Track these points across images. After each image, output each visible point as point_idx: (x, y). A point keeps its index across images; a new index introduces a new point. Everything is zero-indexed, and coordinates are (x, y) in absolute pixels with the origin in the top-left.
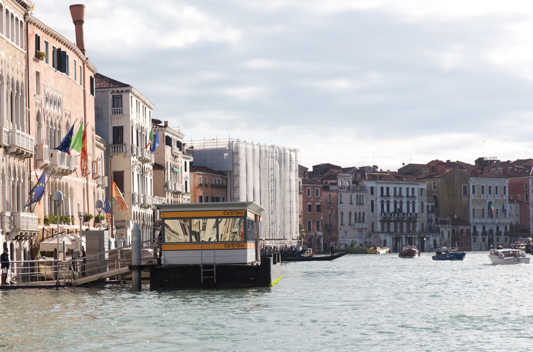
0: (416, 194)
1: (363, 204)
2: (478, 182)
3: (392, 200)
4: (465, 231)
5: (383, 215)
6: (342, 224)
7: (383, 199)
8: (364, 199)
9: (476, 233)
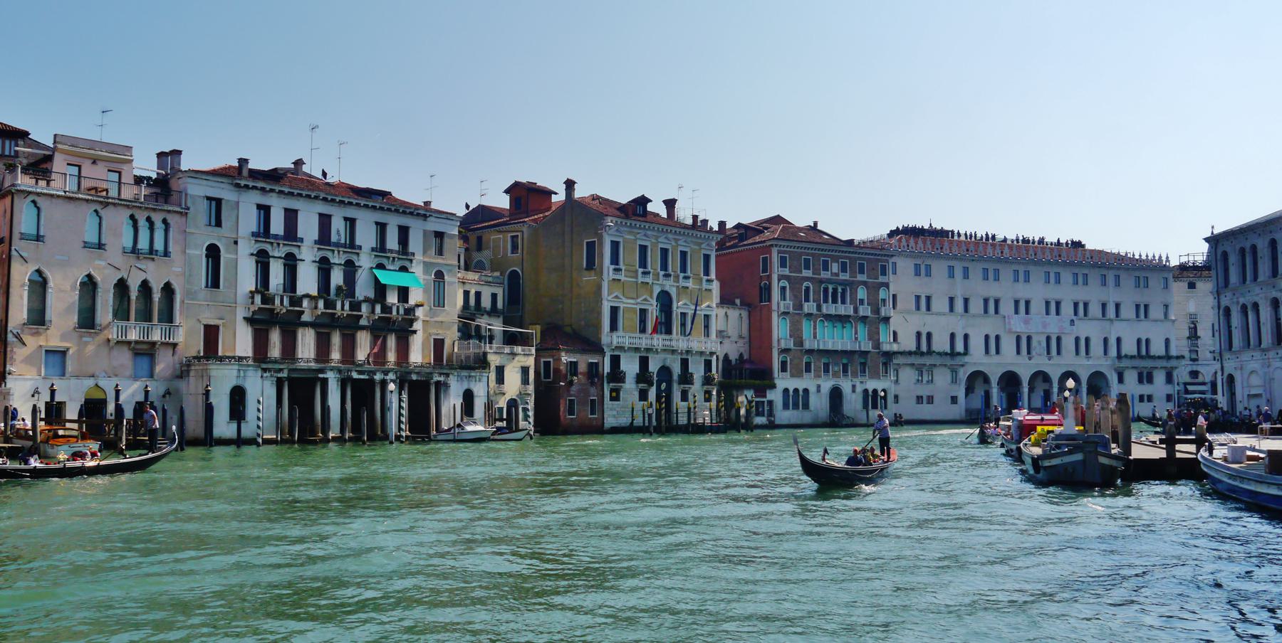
0: (415, 244)
2: (630, 233)
4: (582, 367)
7: (268, 247)
9: (617, 375)
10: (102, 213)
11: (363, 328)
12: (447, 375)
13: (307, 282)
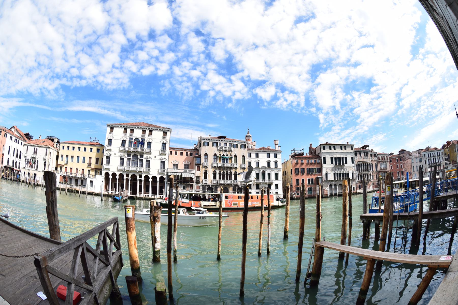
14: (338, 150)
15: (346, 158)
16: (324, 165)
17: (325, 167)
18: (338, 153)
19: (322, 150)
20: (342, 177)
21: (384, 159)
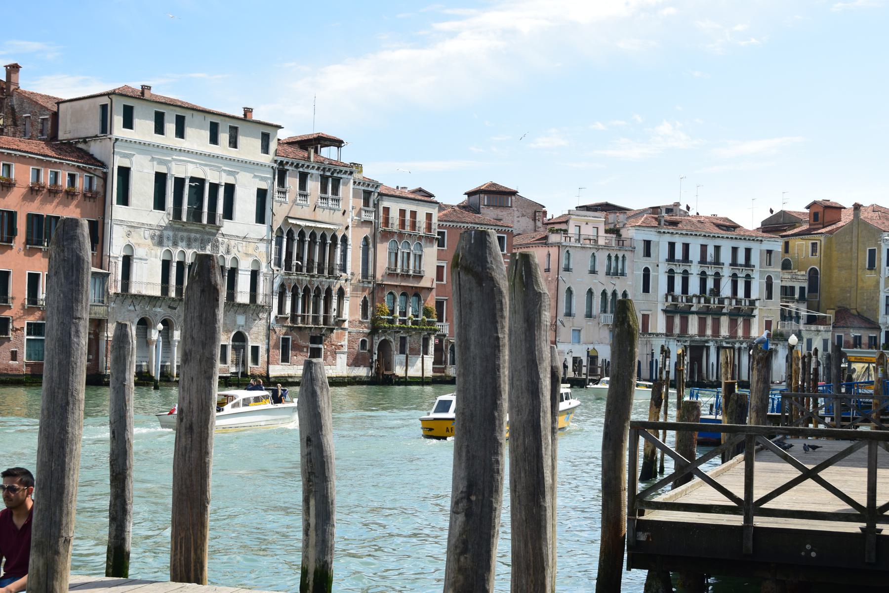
0: (755, 259)
1: (623, 274)
3: (695, 270)
5: (670, 298)
6: (569, 314)
7: (674, 267)
8: (627, 263)
10: (596, 254)
11: (724, 314)
12: (777, 345)
13: (694, 287)
14: (197, 138)
15: (230, 189)
16: (118, 212)
17: (121, 223)
18: (193, 156)
19: (118, 120)
20: (201, 285)
21: (414, 225)
